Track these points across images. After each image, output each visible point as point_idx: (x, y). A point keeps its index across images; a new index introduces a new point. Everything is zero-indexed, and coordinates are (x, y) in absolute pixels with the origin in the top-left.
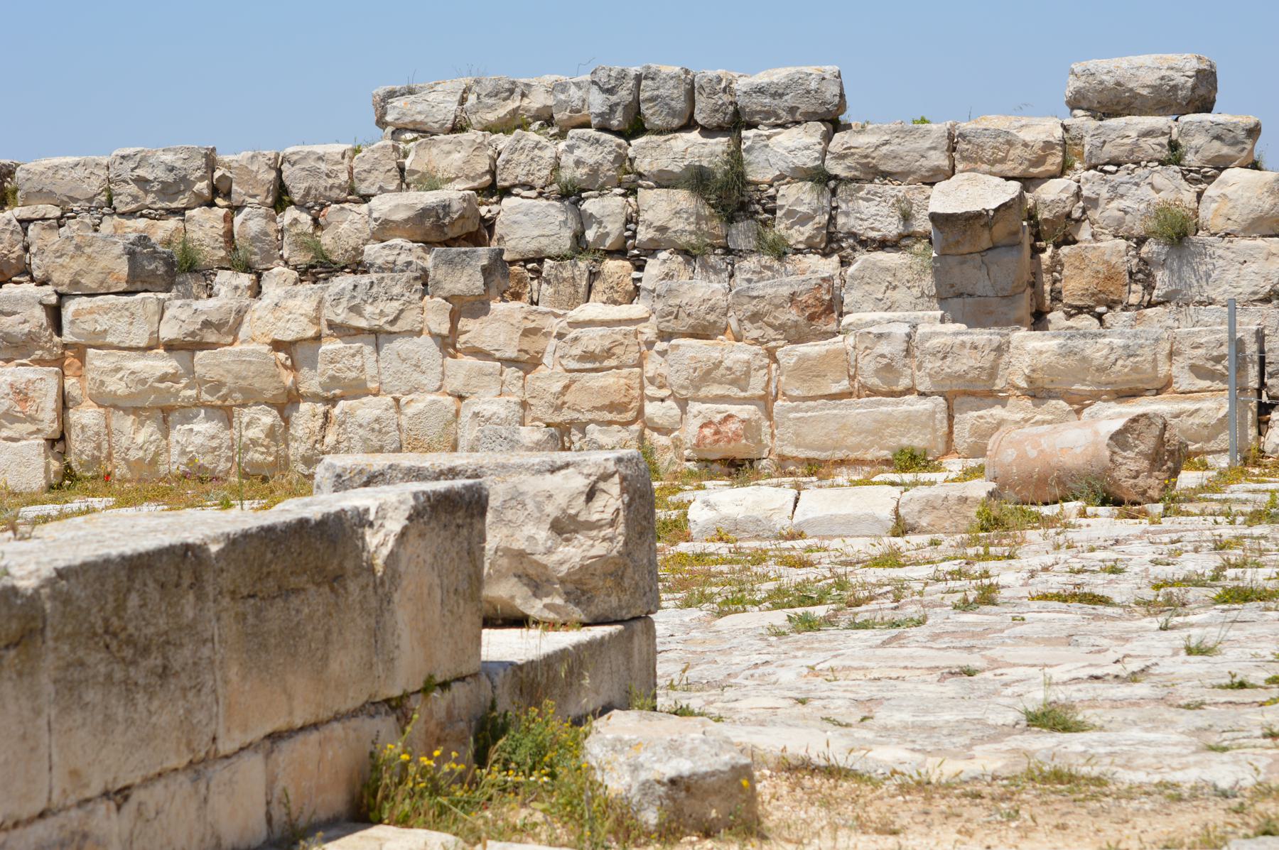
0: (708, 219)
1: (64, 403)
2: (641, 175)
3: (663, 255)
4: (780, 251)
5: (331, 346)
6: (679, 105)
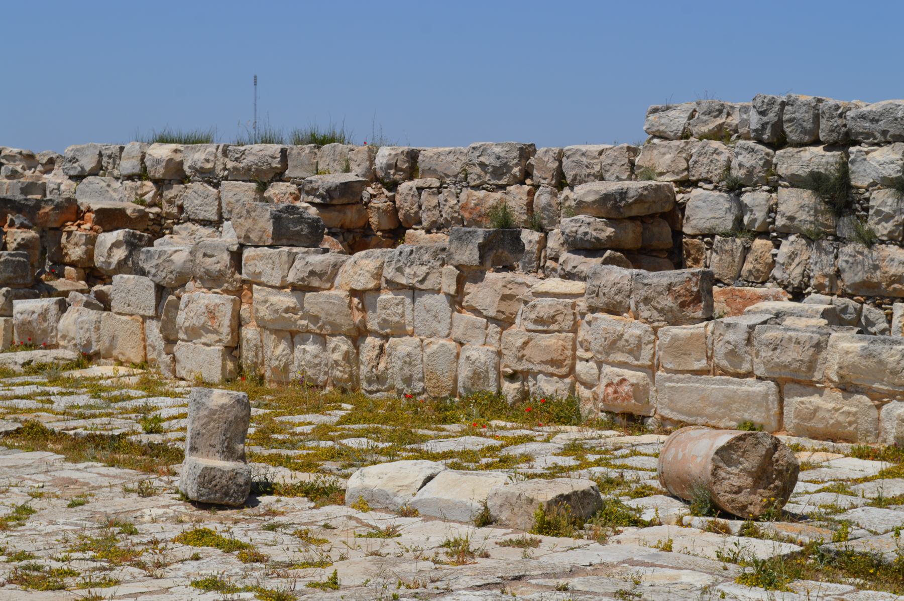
0: (823, 213)
1: (238, 323)
2: (780, 177)
3: (792, 238)
4: (870, 241)
5: (386, 296)
6: (808, 125)
